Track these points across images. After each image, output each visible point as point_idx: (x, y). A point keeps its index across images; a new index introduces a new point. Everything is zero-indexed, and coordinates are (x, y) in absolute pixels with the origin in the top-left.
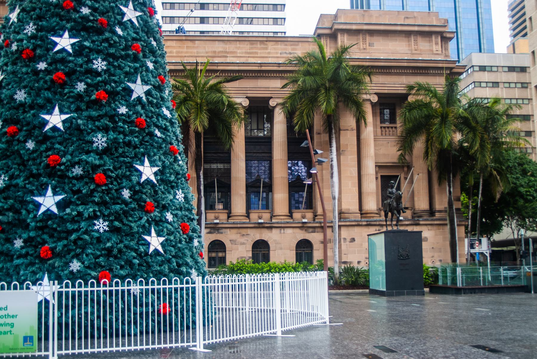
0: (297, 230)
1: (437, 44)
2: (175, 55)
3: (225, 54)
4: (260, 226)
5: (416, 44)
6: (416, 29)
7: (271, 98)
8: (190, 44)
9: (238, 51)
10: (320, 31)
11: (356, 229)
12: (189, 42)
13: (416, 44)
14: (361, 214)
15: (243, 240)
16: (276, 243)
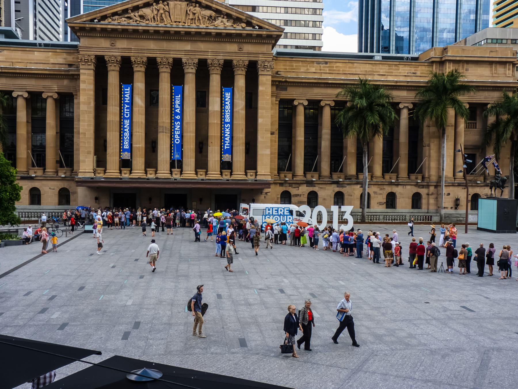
0: (413, 187)
2: (341, 72)
4: (391, 184)
8: (351, 65)
11: (451, 188)
14: (455, 178)
15: (381, 192)
16: (401, 193)
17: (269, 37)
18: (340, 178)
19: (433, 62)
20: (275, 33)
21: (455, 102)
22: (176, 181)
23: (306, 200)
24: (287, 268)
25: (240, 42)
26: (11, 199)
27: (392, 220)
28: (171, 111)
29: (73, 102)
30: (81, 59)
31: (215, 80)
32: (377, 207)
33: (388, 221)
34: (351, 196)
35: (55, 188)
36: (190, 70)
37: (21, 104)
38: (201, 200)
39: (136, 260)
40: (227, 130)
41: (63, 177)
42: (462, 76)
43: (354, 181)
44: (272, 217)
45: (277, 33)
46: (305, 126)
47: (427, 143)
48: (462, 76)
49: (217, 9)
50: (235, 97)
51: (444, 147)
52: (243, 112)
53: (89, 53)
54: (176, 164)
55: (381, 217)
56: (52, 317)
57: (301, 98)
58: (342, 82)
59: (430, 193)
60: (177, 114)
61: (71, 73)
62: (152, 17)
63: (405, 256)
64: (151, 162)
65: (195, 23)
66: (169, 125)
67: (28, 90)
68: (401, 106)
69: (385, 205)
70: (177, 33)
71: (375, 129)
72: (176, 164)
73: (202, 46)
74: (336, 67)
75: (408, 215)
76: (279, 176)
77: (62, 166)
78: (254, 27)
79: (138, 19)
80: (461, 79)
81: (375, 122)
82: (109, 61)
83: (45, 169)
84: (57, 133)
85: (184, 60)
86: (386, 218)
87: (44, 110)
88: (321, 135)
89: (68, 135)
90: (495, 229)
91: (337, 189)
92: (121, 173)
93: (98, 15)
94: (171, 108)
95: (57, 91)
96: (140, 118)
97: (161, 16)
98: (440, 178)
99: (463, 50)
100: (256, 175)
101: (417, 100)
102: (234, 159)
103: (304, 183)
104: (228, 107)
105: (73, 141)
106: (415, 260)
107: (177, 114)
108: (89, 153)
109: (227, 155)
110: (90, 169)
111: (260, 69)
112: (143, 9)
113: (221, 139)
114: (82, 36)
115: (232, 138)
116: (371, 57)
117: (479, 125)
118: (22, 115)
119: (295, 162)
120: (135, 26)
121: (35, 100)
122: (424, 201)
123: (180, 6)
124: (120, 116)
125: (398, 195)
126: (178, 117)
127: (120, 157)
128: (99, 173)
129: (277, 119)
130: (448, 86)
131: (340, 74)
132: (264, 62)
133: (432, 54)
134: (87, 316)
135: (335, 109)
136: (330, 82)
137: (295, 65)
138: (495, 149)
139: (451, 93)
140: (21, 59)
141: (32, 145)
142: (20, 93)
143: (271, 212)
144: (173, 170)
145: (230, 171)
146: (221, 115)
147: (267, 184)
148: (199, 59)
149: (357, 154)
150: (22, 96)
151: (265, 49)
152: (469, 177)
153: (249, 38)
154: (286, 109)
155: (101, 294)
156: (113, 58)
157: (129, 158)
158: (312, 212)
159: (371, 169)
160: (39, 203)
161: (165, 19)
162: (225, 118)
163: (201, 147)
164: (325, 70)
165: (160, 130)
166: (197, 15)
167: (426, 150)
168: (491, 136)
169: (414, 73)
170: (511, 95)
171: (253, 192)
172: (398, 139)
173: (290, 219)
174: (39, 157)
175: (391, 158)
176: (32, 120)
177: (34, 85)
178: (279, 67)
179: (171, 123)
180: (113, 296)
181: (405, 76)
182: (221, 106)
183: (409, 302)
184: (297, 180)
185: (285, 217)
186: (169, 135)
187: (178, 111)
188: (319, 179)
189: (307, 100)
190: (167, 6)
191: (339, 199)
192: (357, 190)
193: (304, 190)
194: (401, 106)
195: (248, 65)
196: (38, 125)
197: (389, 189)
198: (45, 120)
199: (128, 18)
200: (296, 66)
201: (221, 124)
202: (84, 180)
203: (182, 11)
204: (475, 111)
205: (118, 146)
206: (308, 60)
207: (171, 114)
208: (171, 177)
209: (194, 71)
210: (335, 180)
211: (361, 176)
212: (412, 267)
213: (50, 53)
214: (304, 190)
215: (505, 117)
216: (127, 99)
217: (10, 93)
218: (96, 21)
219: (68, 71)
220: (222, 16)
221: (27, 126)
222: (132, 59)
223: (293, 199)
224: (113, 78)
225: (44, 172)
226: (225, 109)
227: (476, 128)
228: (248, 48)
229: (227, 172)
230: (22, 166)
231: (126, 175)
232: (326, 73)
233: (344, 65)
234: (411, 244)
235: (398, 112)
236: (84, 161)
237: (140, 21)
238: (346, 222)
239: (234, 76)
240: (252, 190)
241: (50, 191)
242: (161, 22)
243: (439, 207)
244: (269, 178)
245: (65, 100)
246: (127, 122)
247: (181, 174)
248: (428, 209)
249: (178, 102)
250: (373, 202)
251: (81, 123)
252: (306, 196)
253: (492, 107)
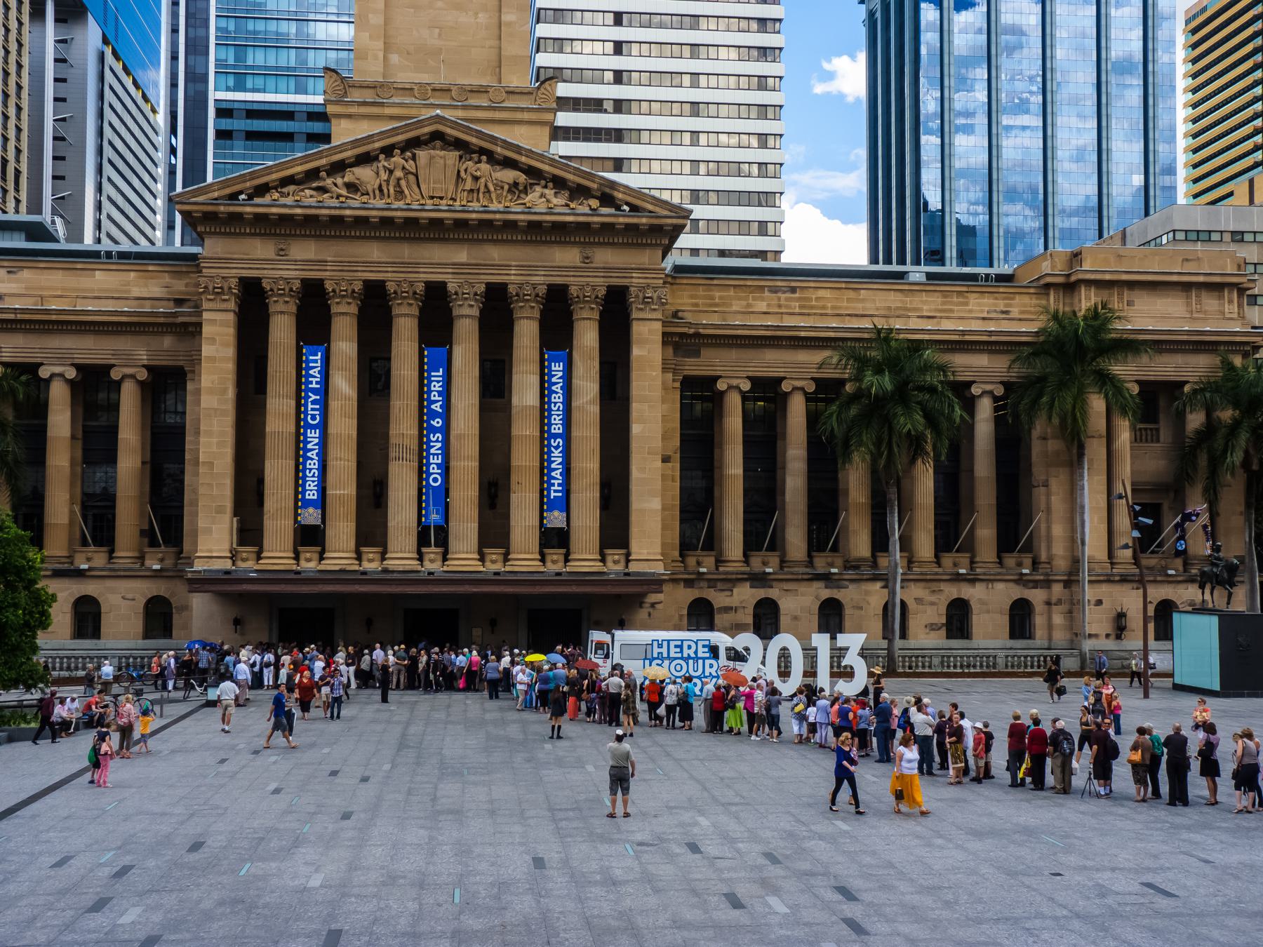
0: (1011, 585)
1: (1231, 302)
2: (829, 311)
3: (903, 314)
4: (957, 578)
5: (1199, 302)
6: (1201, 279)
7: (974, 382)
8: (851, 294)
10: (1049, 280)
11: (1105, 588)
13: (1199, 302)
14: (1112, 564)
15: (933, 598)
16: (982, 602)
17: (656, 230)
18: (832, 565)
19: (1048, 286)
20: (669, 221)
21: (1106, 381)
22: (431, 577)
23: (750, 620)
24: (705, 789)
25: (585, 243)
26: (27, 624)
27: (962, 667)
28: (421, 407)
29: (185, 389)
30: (206, 287)
31: (527, 333)
32: (925, 636)
33: (952, 670)
34: (861, 608)
35: (138, 596)
36: (466, 311)
37: (59, 395)
38: (493, 623)
39: (334, 773)
40: (556, 453)
41: (156, 570)
42: (1119, 318)
43: (867, 572)
44: (667, 662)
45: (675, 221)
46: (744, 442)
47: (1043, 477)
48: (1119, 318)
49: (530, 167)
50: (574, 374)
51: (1083, 489)
52: (595, 409)
53: (225, 272)
54: (433, 536)
55: (936, 661)
56: (121, 921)
57: (733, 373)
58: (832, 335)
59: (1054, 600)
60: (434, 415)
61: (180, 319)
62: (376, 186)
63: (999, 756)
64: (371, 531)
65: (478, 200)
66: (416, 441)
67: (76, 361)
68: (975, 390)
69: (943, 632)
70: (436, 224)
71: (915, 446)
72: (433, 536)
73: (495, 253)
74: (817, 299)
75: (1001, 654)
76: (682, 562)
77: (153, 543)
78: (618, 208)
79: (344, 192)
80: (1118, 326)
81: (916, 430)
82: (272, 290)
83: (112, 551)
84: (143, 463)
85: (451, 287)
86: (948, 662)
87: (114, 408)
88: (784, 463)
89: (171, 467)
90: (1217, 687)
91: (826, 594)
92: (297, 558)
93: (248, 184)
94: (421, 399)
95: (145, 362)
96: (344, 424)
97: (398, 185)
98: (1076, 562)
99: (1120, 256)
100: (628, 561)
101: (1013, 376)
102: (574, 523)
103: (745, 580)
104: (558, 398)
105: (182, 482)
106: (1024, 766)
107: (434, 415)
108: (220, 510)
109: (556, 513)
111: (634, 306)
112: (354, 169)
113: (542, 475)
114: (210, 233)
115: (567, 472)
116: (901, 275)
117: (1165, 433)
118: (60, 420)
119: (721, 529)
120: (335, 208)
121: (93, 386)
122: (1039, 620)
123: (442, 161)
124: (298, 420)
125: (975, 606)
126: (437, 423)
127: (296, 521)
128: (244, 560)
129: (677, 424)
130: (1087, 341)
131: (826, 315)
132: (643, 289)
133: (1046, 267)
134: (208, 916)
135: (817, 400)
136: (803, 334)
137: (717, 294)
138: (1206, 490)
139: (1093, 359)
140: (64, 289)
141: (84, 494)
142: (57, 370)
143: (664, 650)
144: (424, 550)
145: (563, 551)
146: (542, 417)
147: (655, 583)
148: (487, 284)
149: (873, 507)
150: (61, 375)
151: (644, 258)
152: (1149, 561)
153: (606, 234)
154: (699, 402)
155: (245, 861)
156: (282, 285)
157: (319, 523)
158: (765, 649)
159: (906, 544)
160: (96, 634)
161: (406, 192)
162: (550, 425)
163: (494, 493)
165: (392, 454)
166: (483, 180)
167: (1039, 494)
168: (1194, 462)
169: (1003, 312)
170: (1238, 361)
171: (621, 603)
172: (971, 471)
173: (712, 667)
174: (98, 521)
175: (957, 514)
176: (84, 432)
177: (92, 350)
178: (680, 301)
179: (421, 436)
180: (274, 865)
181: (984, 319)
182: (542, 396)
183: (1012, 874)
184: (727, 573)
185: (700, 662)
186: (416, 464)
187: (437, 407)
188: (782, 568)
190: (411, 162)
191: (831, 617)
192: (875, 595)
193: (746, 596)
194: (975, 390)
195: (606, 296)
196: (97, 444)
197: (953, 591)
198: (117, 433)
199: (318, 189)
200: (721, 298)
201: (542, 439)
202: (207, 576)
203: (449, 174)
204: (1155, 401)
205: (292, 492)
206: (749, 283)
207: (421, 414)
208: (419, 568)
209: (475, 312)
210: (821, 571)
211: (883, 561)
212: (1016, 784)
213: (132, 274)
214: (746, 596)
215: (1226, 415)
216: (314, 380)
217: (33, 368)
218: (243, 197)
219: (174, 315)
220: (543, 182)
221: (73, 447)
222: (327, 286)
223: (718, 619)
224: (282, 331)
225: (111, 558)
226: (550, 402)
227: (1158, 441)
228: (605, 256)
229: (555, 555)
230: (56, 546)
231: (309, 564)
233: (835, 294)
234: (1013, 727)
235: (970, 405)
236: (208, 531)
237: (347, 198)
238: (848, 674)
239: (572, 322)
240: (618, 597)
241: (122, 604)
242: (396, 199)
243: (1076, 634)
244: (659, 569)
245: (166, 385)
246: (313, 436)
247: (445, 559)
248: (1050, 639)
249: (436, 387)
250: (915, 624)
251: (202, 439)
252: (750, 610)
253: (1195, 391)
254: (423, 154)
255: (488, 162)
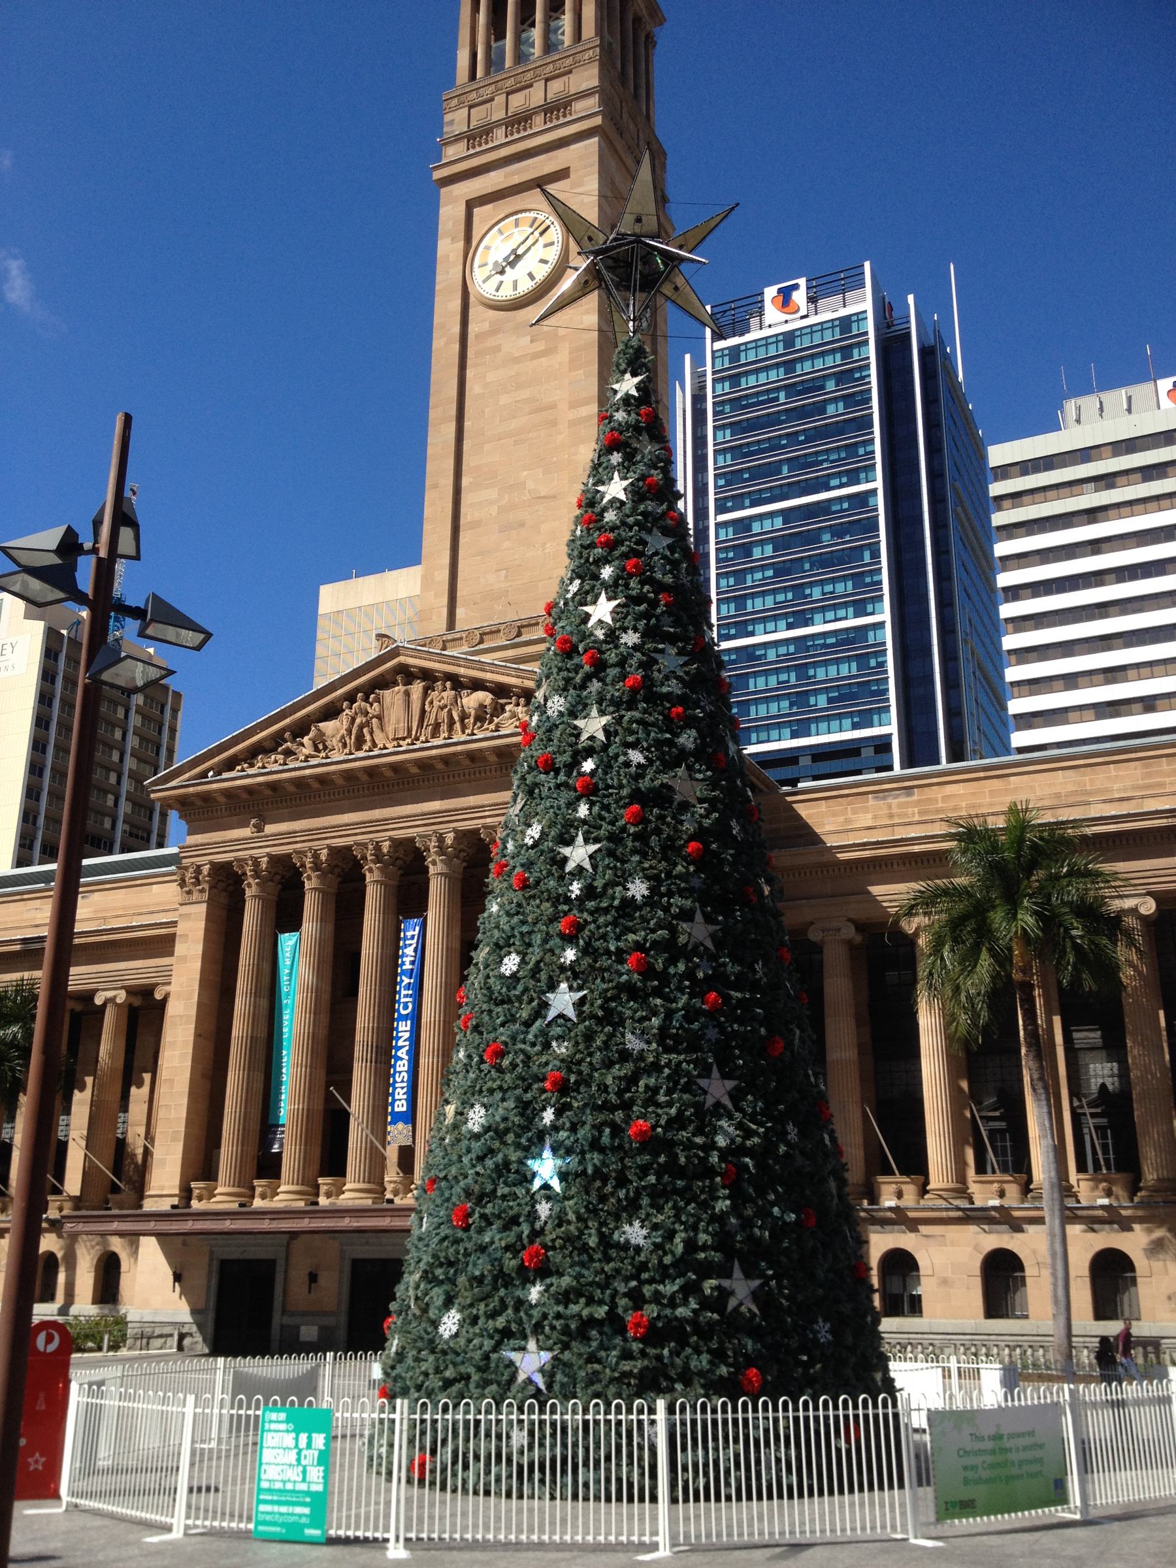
9: (1116, 786)
12: (996, 780)
74: (945, 798)
110: (171, 1187)
136: (917, 848)
142: (110, 994)
164: (906, 815)
189: (849, 920)
190: (375, 704)
218: (211, 773)
232: (910, 824)
254: (387, 694)
255: (452, 689)
